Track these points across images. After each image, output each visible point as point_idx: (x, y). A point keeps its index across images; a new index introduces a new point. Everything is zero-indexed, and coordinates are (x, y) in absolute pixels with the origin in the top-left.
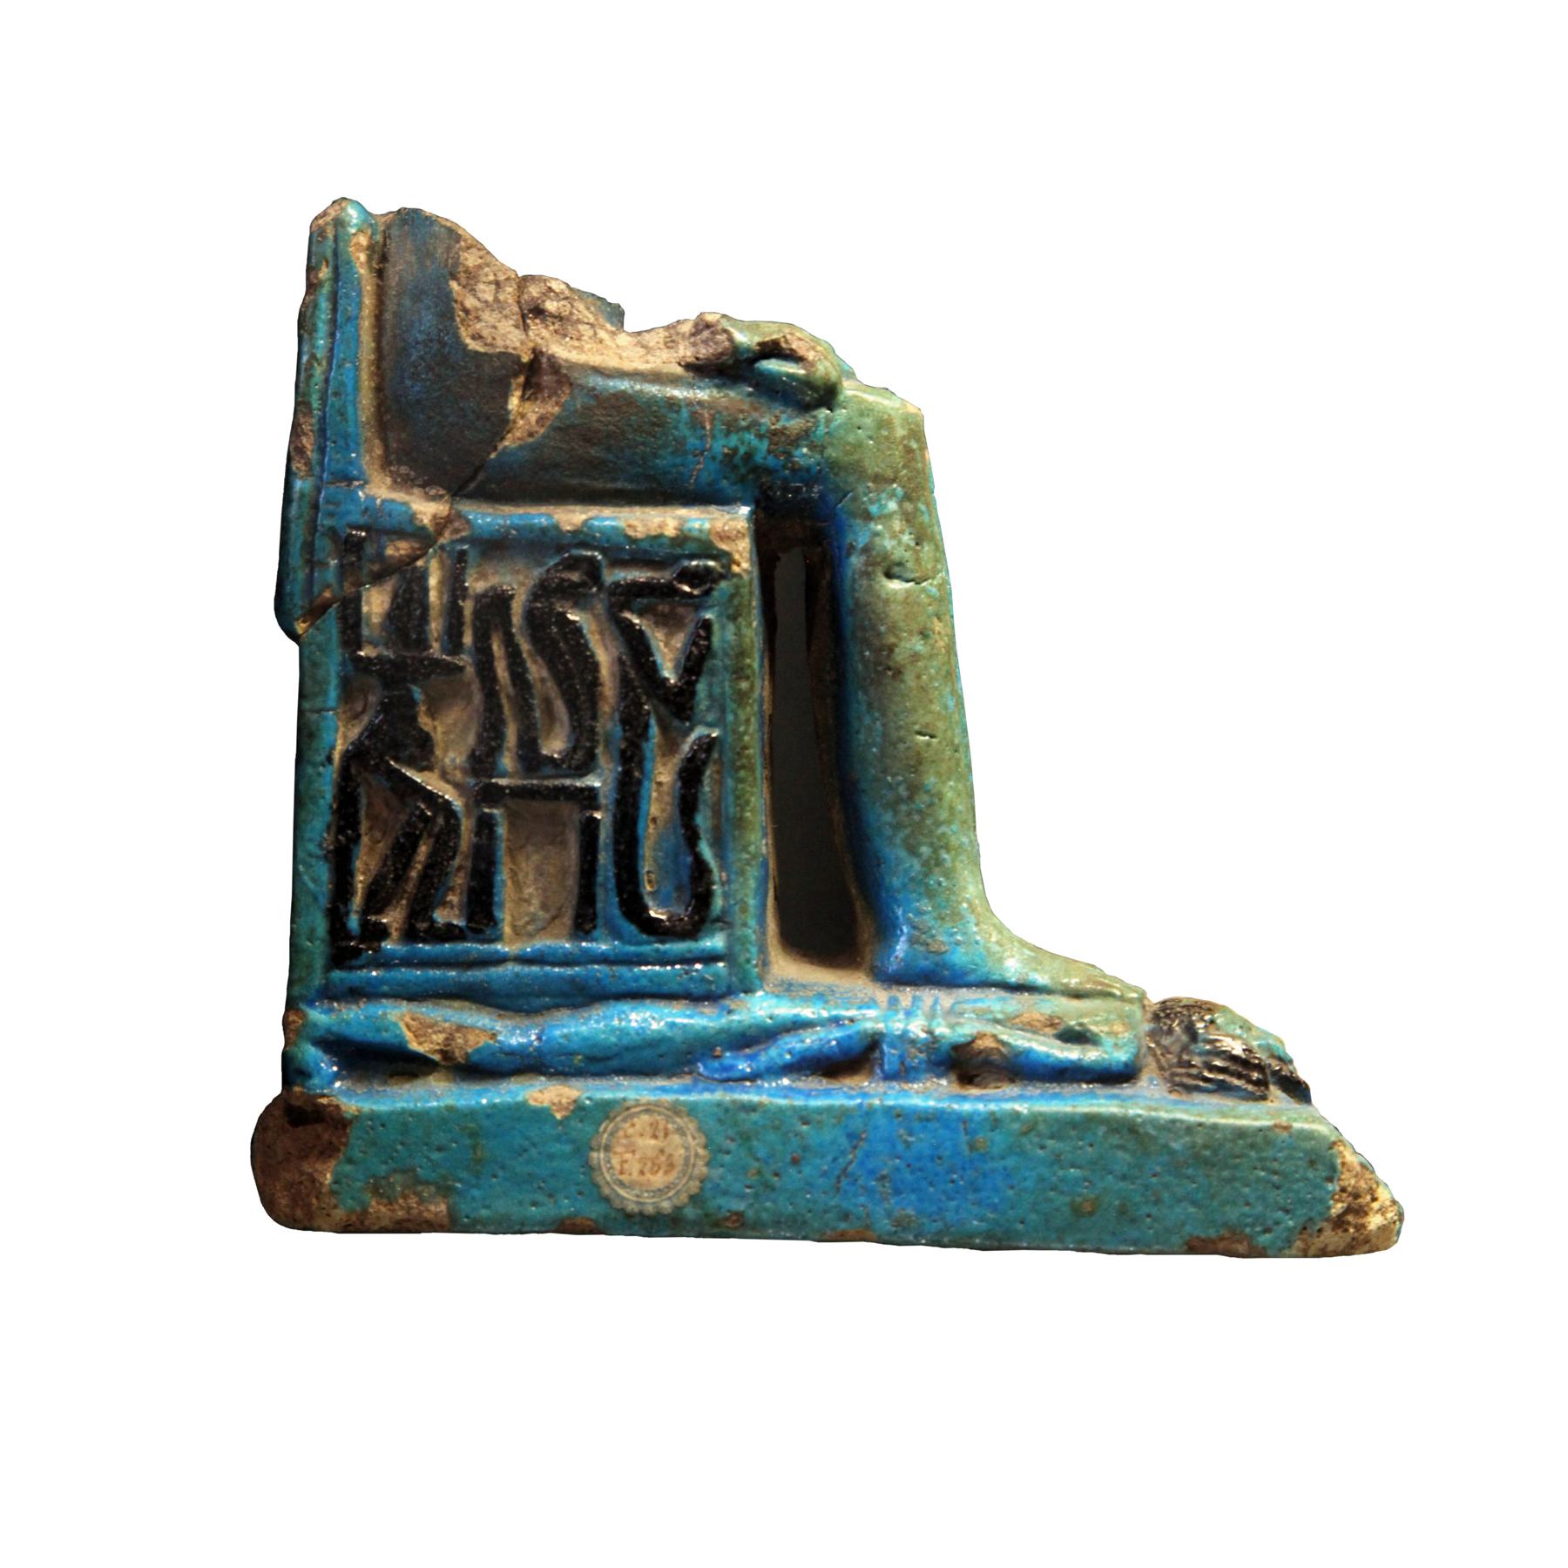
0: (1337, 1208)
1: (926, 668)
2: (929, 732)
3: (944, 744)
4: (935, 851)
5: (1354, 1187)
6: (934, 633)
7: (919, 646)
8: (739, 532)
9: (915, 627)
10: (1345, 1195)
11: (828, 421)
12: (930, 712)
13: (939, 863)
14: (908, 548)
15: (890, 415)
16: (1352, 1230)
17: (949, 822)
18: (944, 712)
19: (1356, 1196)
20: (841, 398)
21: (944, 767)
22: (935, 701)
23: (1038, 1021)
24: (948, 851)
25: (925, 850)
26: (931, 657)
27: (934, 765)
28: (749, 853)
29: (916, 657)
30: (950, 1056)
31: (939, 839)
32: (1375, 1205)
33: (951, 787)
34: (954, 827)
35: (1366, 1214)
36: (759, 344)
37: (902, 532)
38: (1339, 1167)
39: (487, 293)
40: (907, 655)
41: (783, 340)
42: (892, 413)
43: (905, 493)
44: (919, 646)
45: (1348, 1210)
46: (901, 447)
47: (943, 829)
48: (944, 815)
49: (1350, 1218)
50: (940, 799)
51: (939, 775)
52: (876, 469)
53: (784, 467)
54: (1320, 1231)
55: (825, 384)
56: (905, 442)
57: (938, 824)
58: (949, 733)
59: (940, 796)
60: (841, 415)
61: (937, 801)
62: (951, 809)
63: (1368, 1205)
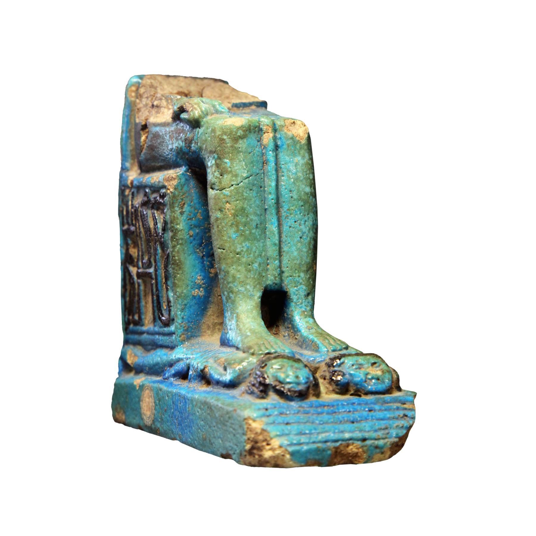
0: (248, 447)
1: (221, 223)
2: (222, 248)
3: (229, 251)
4: (228, 294)
5: (253, 438)
6: (225, 209)
7: (219, 215)
8: (172, 177)
9: (217, 207)
10: (249, 441)
11: (198, 132)
12: (222, 240)
13: (230, 298)
14: (217, 178)
15: (215, 127)
16: (257, 457)
17: (233, 282)
18: (229, 240)
19: (256, 442)
20: (202, 123)
21: (229, 261)
22: (224, 236)
23: (222, 361)
24: (232, 293)
25: (226, 293)
26: (224, 219)
27: (224, 260)
28: (176, 295)
29: (217, 219)
30: (200, 374)
31: (229, 289)
32: (268, 447)
33: (233, 268)
34: (236, 284)
35: (261, 450)
36: (178, 108)
37: (215, 172)
38: (246, 429)
39: (144, 101)
40: (214, 219)
41: (184, 105)
42: (216, 127)
43: (218, 157)
44: (219, 215)
45: (253, 448)
46: (218, 139)
47: (231, 285)
48: (230, 280)
49: (255, 451)
50: (228, 273)
51: (227, 264)
52: (210, 149)
53: (190, 151)
54: (246, 456)
55: (194, 120)
56: (220, 137)
57: (228, 283)
58: (233, 248)
59: (228, 272)
60: (201, 130)
61: (226, 274)
62: (234, 277)
63: (263, 446)
